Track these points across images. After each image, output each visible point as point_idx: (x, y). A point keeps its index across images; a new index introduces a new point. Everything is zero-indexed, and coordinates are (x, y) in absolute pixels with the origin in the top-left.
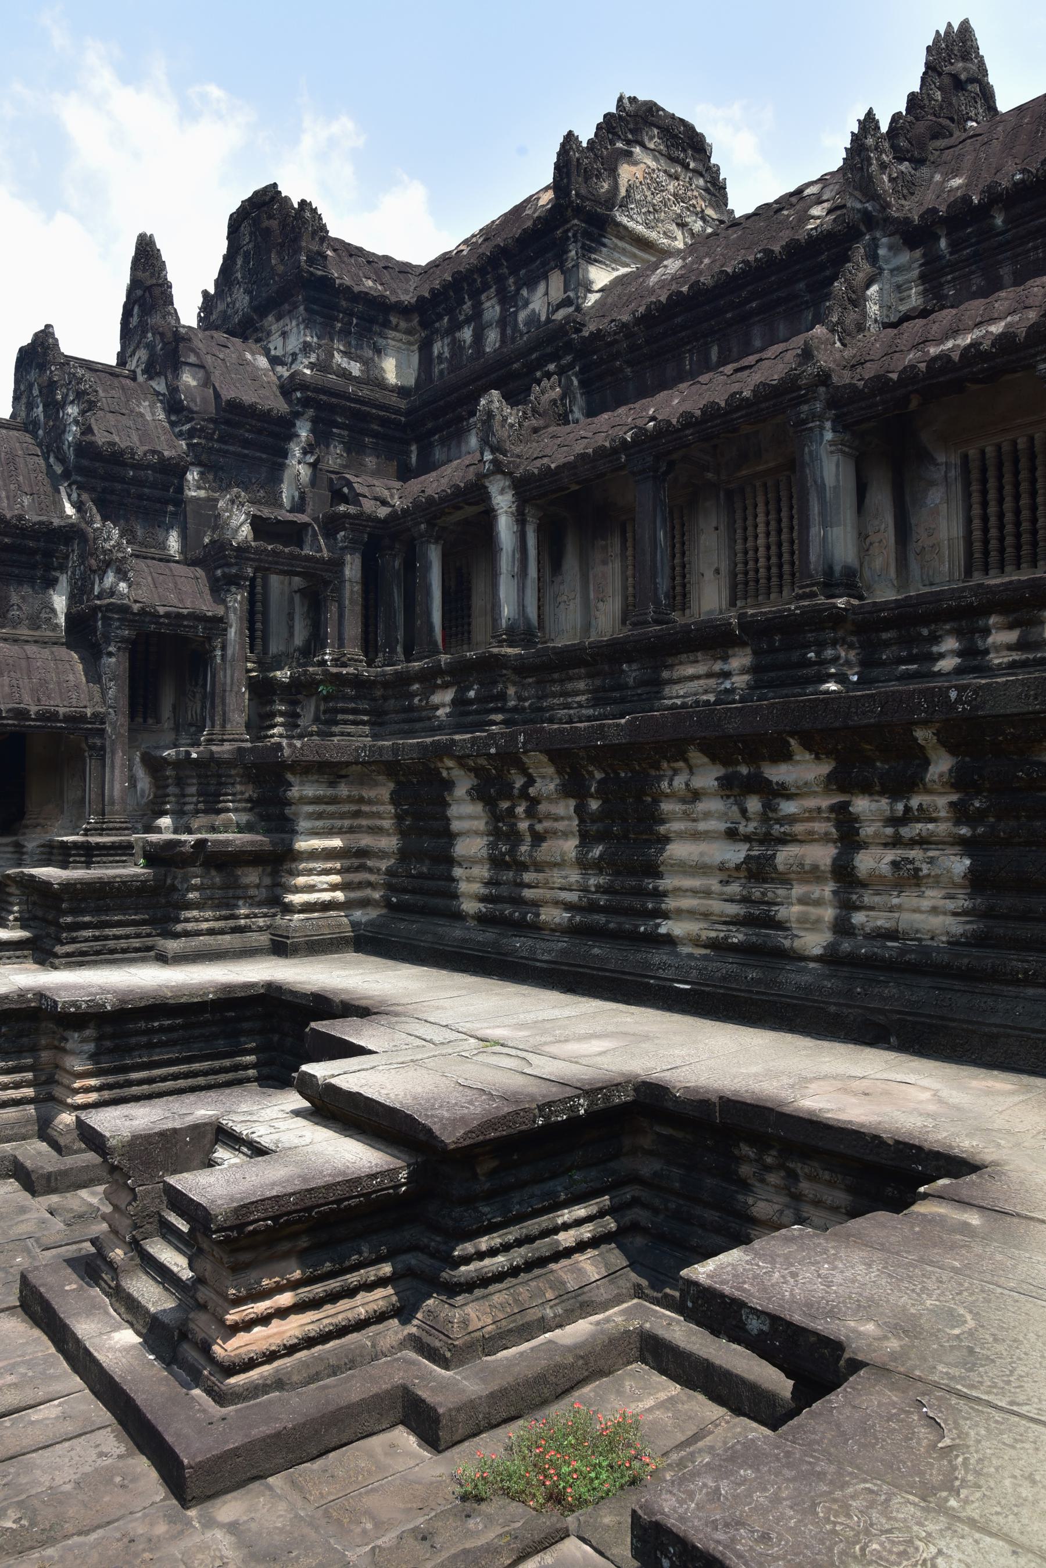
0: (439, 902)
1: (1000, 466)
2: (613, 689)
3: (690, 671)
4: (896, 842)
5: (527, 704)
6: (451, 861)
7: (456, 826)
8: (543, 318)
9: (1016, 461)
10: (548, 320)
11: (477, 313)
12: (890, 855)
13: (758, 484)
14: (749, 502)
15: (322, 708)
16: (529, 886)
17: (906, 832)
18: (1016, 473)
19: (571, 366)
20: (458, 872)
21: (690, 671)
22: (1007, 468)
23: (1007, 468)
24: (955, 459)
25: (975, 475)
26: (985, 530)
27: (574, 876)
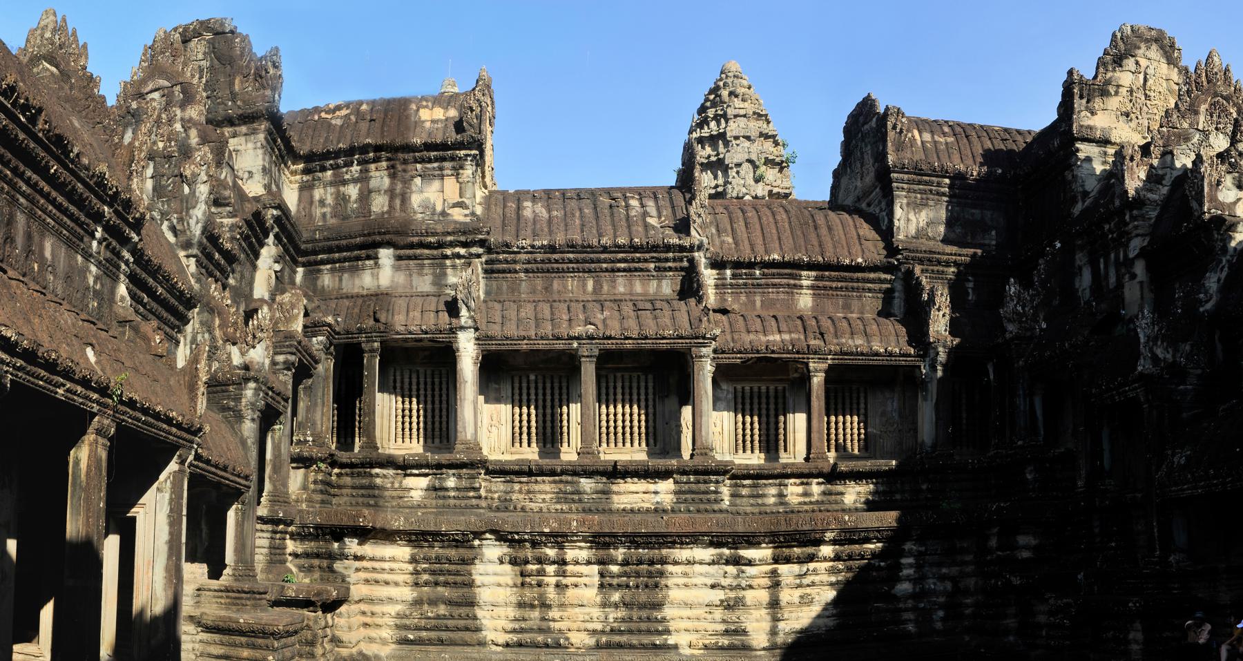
0: (467, 636)
1: (751, 398)
2: (573, 493)
3: (633, 487)
4: (800, 586)
5: (496, 496)
6: (471, 603)
7: (478, 579)
8: (439, 208)
9: (759, 397)
10: (444, 213)
11: (363, 178)
12: (800, 592)
13: (619, 375)
14: (611, 385)
15: (311, 479)
16: (554, 620)
17: (806, 581)
18: (760, 404)
19: (479, 256)
20: (479, 613)
21: (633, 487)
22: (756, 401)
23: (756, 401)
24: (731, 389)
25: (740, 400)
26: (744, 430)
27: (596, 612)
